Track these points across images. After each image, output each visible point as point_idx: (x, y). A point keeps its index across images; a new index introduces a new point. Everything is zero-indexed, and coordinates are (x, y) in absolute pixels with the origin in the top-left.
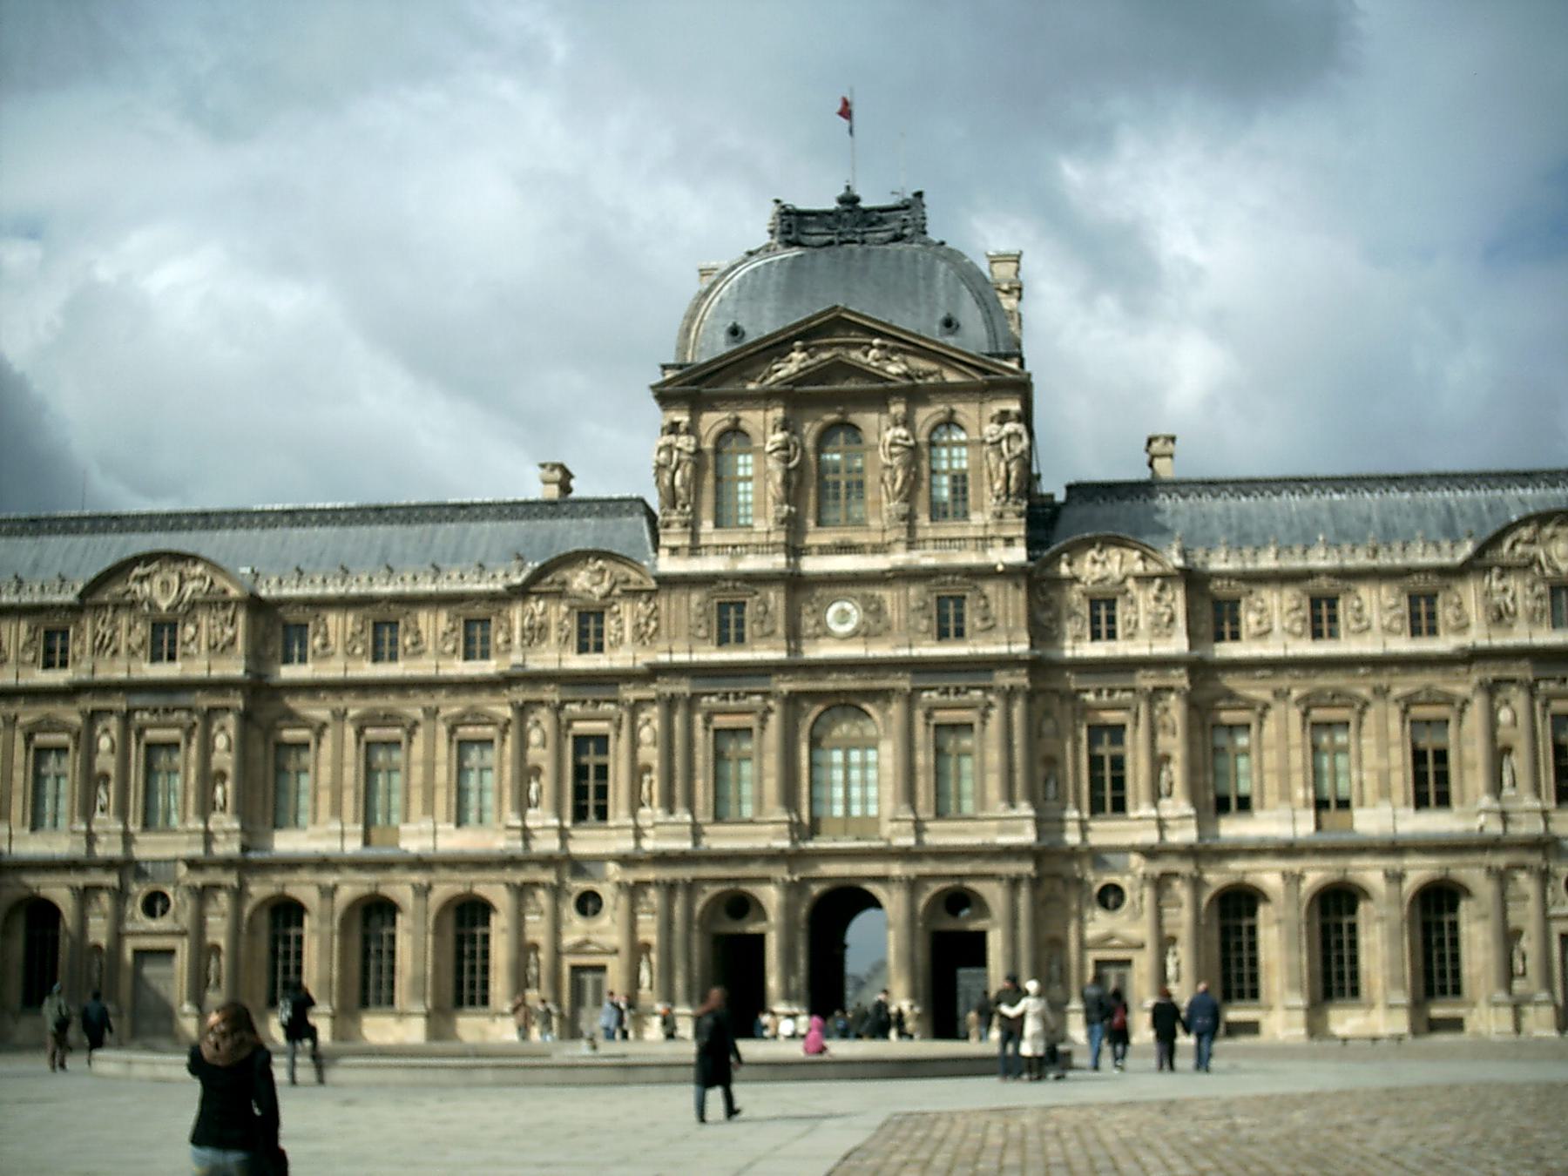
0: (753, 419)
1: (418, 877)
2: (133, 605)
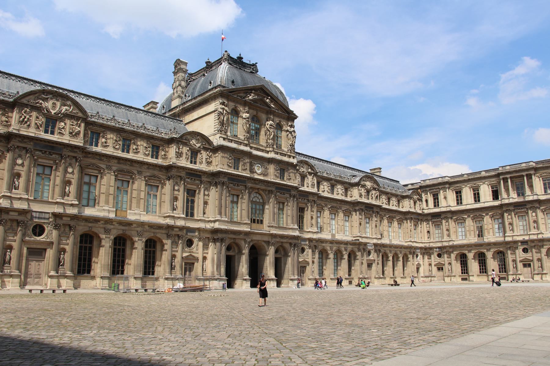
0: (241, 108)
1: (139, 229)
2: (39, 109)
